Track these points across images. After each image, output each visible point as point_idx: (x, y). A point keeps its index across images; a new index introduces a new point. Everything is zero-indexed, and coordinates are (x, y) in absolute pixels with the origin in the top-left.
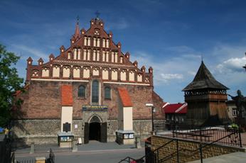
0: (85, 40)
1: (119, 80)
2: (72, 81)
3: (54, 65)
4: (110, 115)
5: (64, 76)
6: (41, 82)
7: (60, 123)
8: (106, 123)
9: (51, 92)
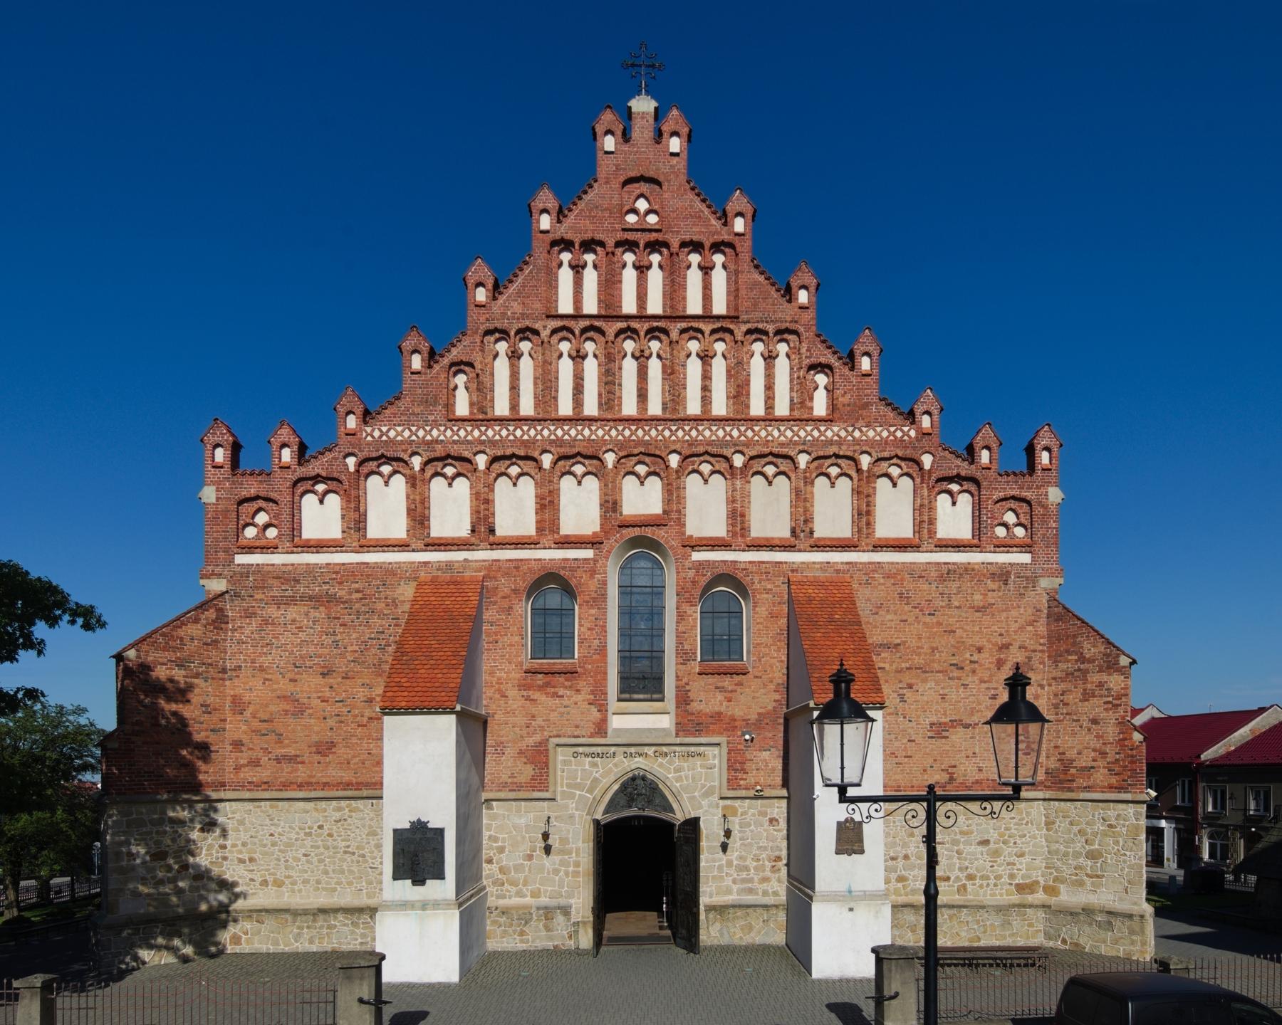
0: (565, 276)
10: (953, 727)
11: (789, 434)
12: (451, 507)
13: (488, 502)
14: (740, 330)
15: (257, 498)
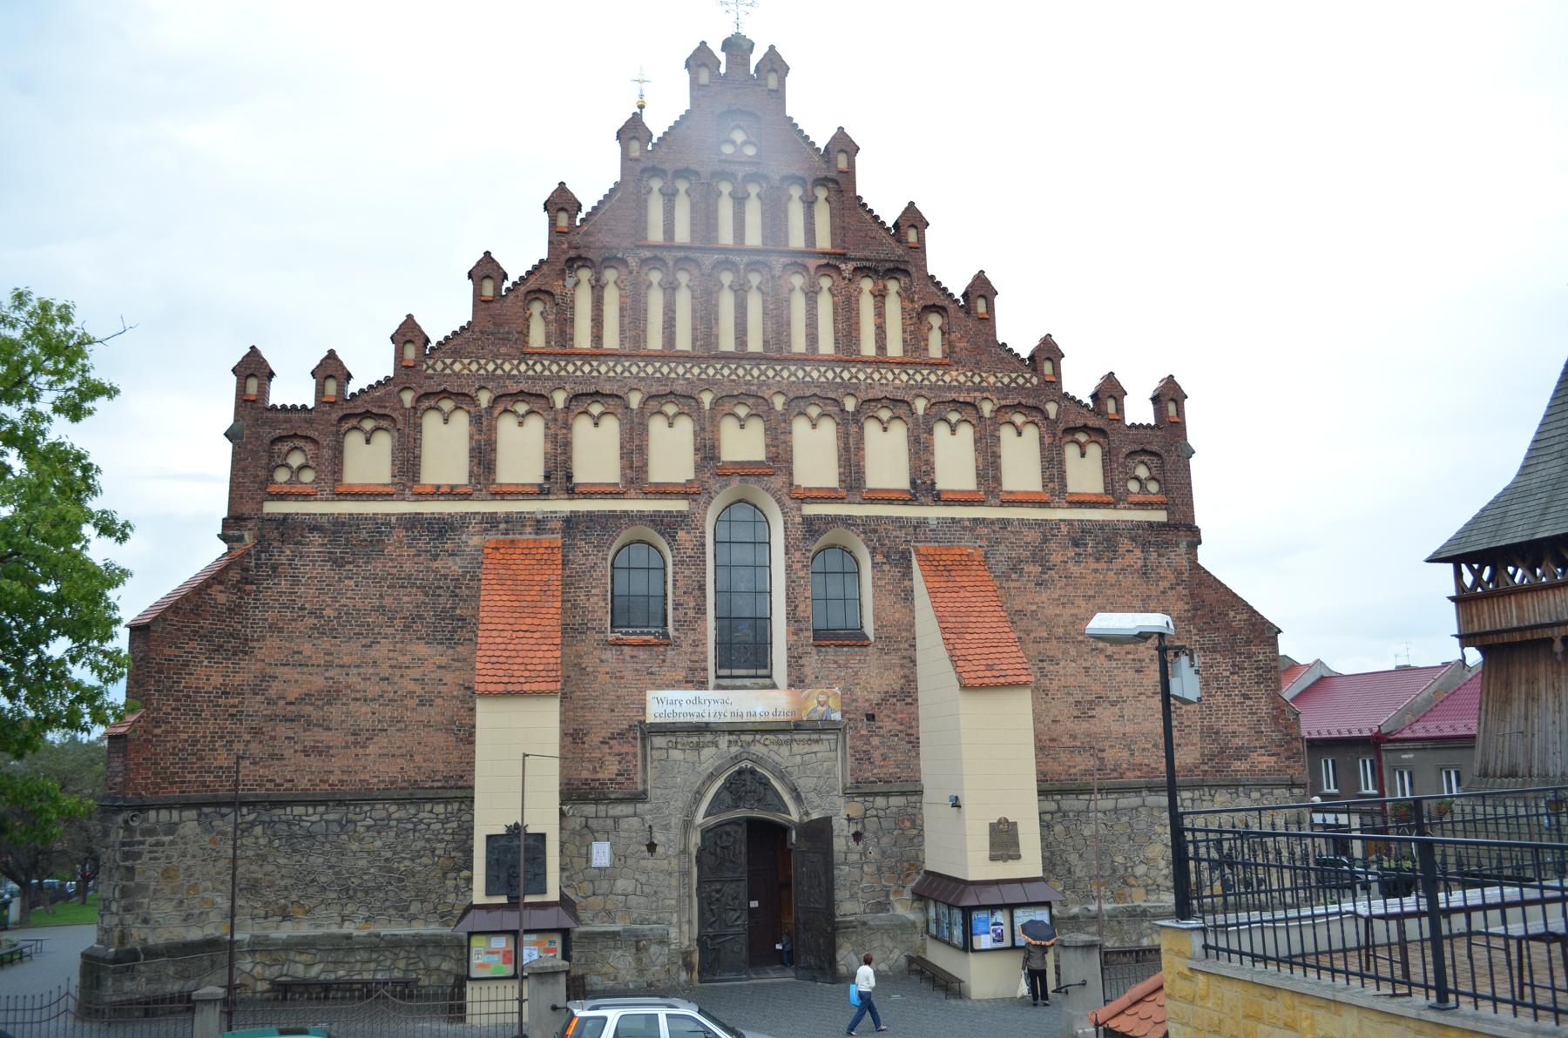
1: (922, 488)
2: (565, 506)
3: (430, 397)
4: (863, 758)
5: (507, 473)
6: (338, 527)
7: (467, 831)
8: (820, 831)
9: (408, 600)
10: (1098, 704)
11: (904, 377)
12: (521, 448)
13: (567, 445)
14: (847, 268)
15: (295, 435)
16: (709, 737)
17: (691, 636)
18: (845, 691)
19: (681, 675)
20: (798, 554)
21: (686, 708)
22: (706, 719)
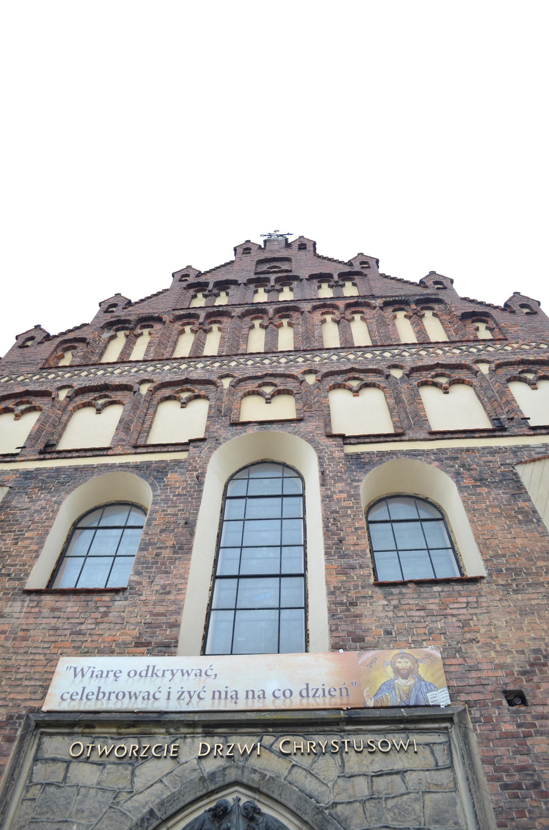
16: (161, 740)
17: (161, 580)
18: (450, 652)
19: (131, 633)
20: (340, 486)
21: (125, 684)
22: (161, 705)
